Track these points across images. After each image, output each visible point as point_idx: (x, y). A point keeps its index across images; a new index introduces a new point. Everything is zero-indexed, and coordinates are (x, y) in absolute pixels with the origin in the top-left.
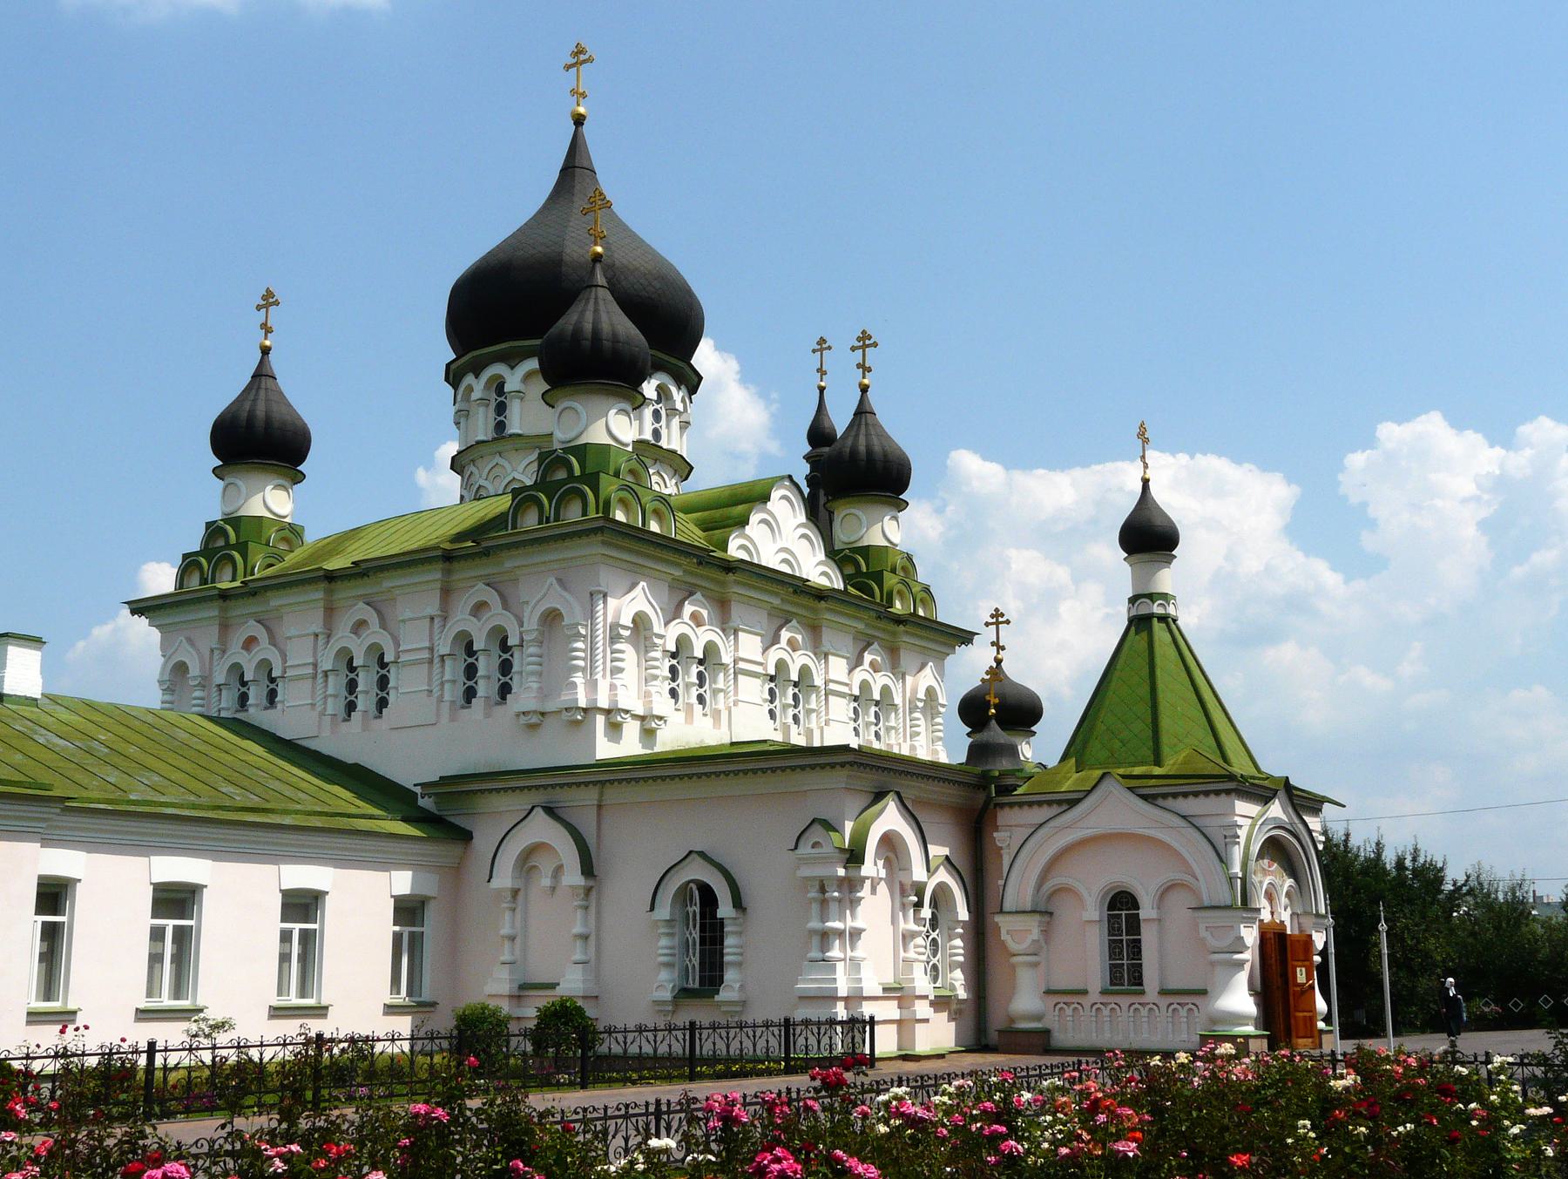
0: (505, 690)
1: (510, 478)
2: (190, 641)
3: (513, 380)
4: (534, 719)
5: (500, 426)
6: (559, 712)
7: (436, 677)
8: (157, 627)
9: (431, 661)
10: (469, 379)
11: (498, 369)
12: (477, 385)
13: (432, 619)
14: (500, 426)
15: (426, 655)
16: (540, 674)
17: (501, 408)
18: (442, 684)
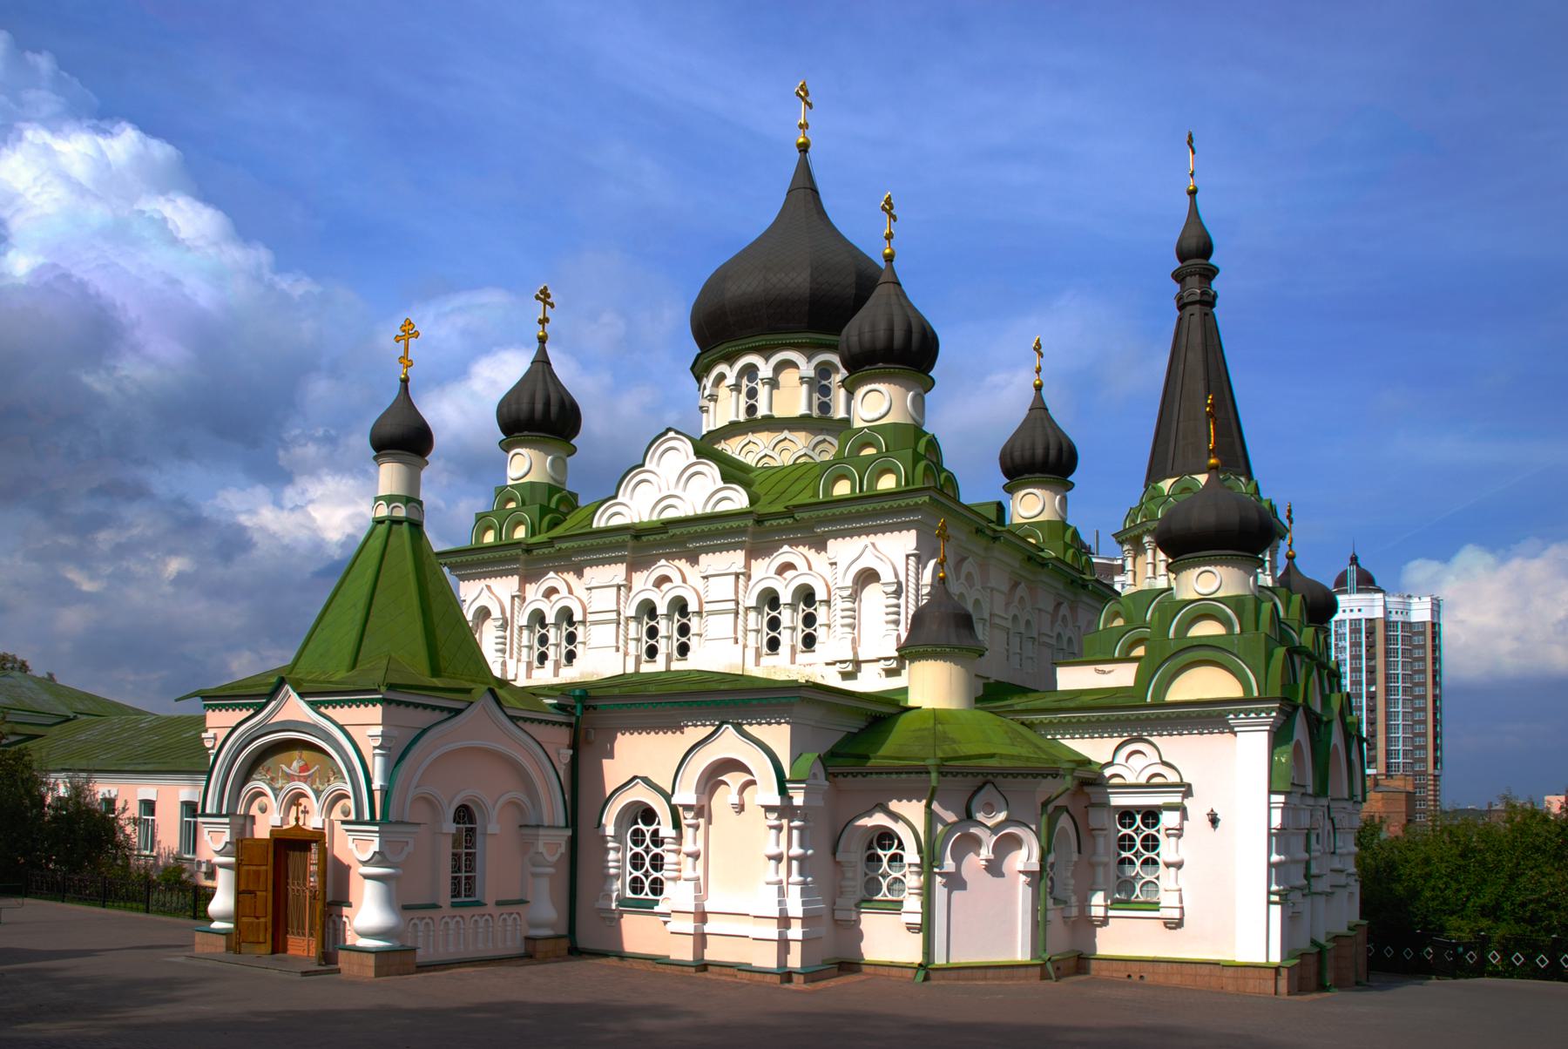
0: (809, 641)
1: (762, 454)
2: (488, 587)
3: (765, 369)
4: (850, 668)
5: (751, 409)
6: (878, 660)
7: (740, 628)
8: (457, 576)
9: (737, 613)
10: (722, 368)
11: (752, 359)
12: (731, 373)
13: (737, 576)
14: (751, 409)
15: (732, 605)
16: (852, 626)
17: (752, 393)
18: (746, 631)
